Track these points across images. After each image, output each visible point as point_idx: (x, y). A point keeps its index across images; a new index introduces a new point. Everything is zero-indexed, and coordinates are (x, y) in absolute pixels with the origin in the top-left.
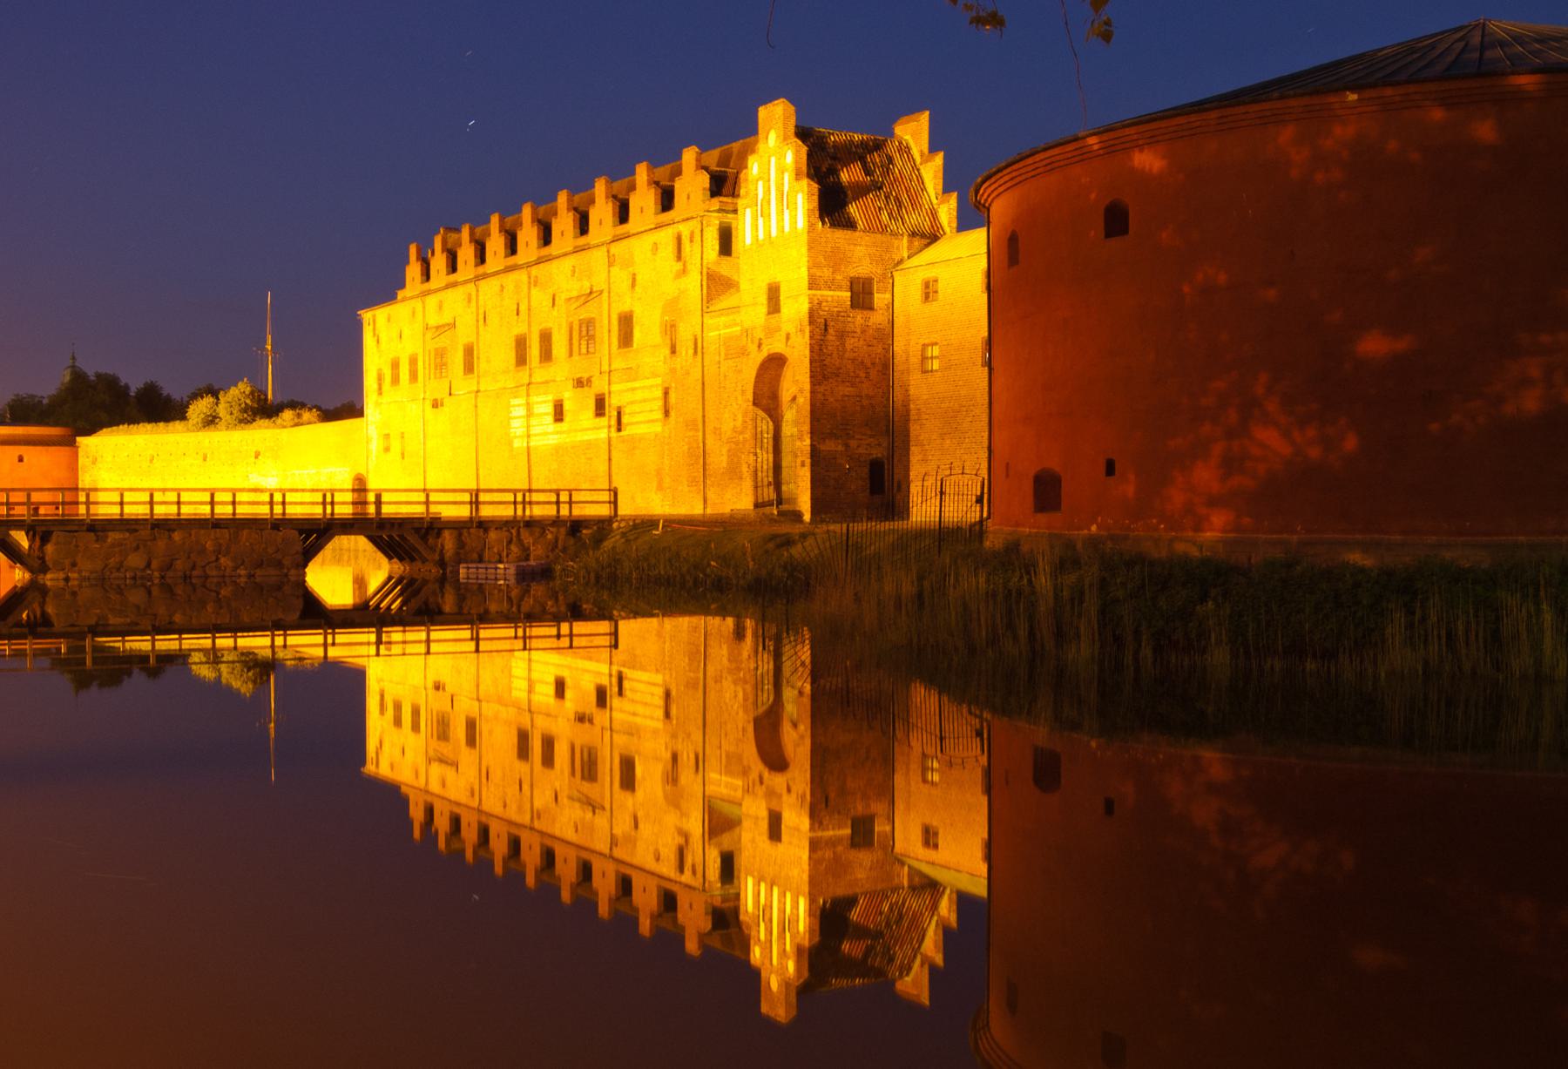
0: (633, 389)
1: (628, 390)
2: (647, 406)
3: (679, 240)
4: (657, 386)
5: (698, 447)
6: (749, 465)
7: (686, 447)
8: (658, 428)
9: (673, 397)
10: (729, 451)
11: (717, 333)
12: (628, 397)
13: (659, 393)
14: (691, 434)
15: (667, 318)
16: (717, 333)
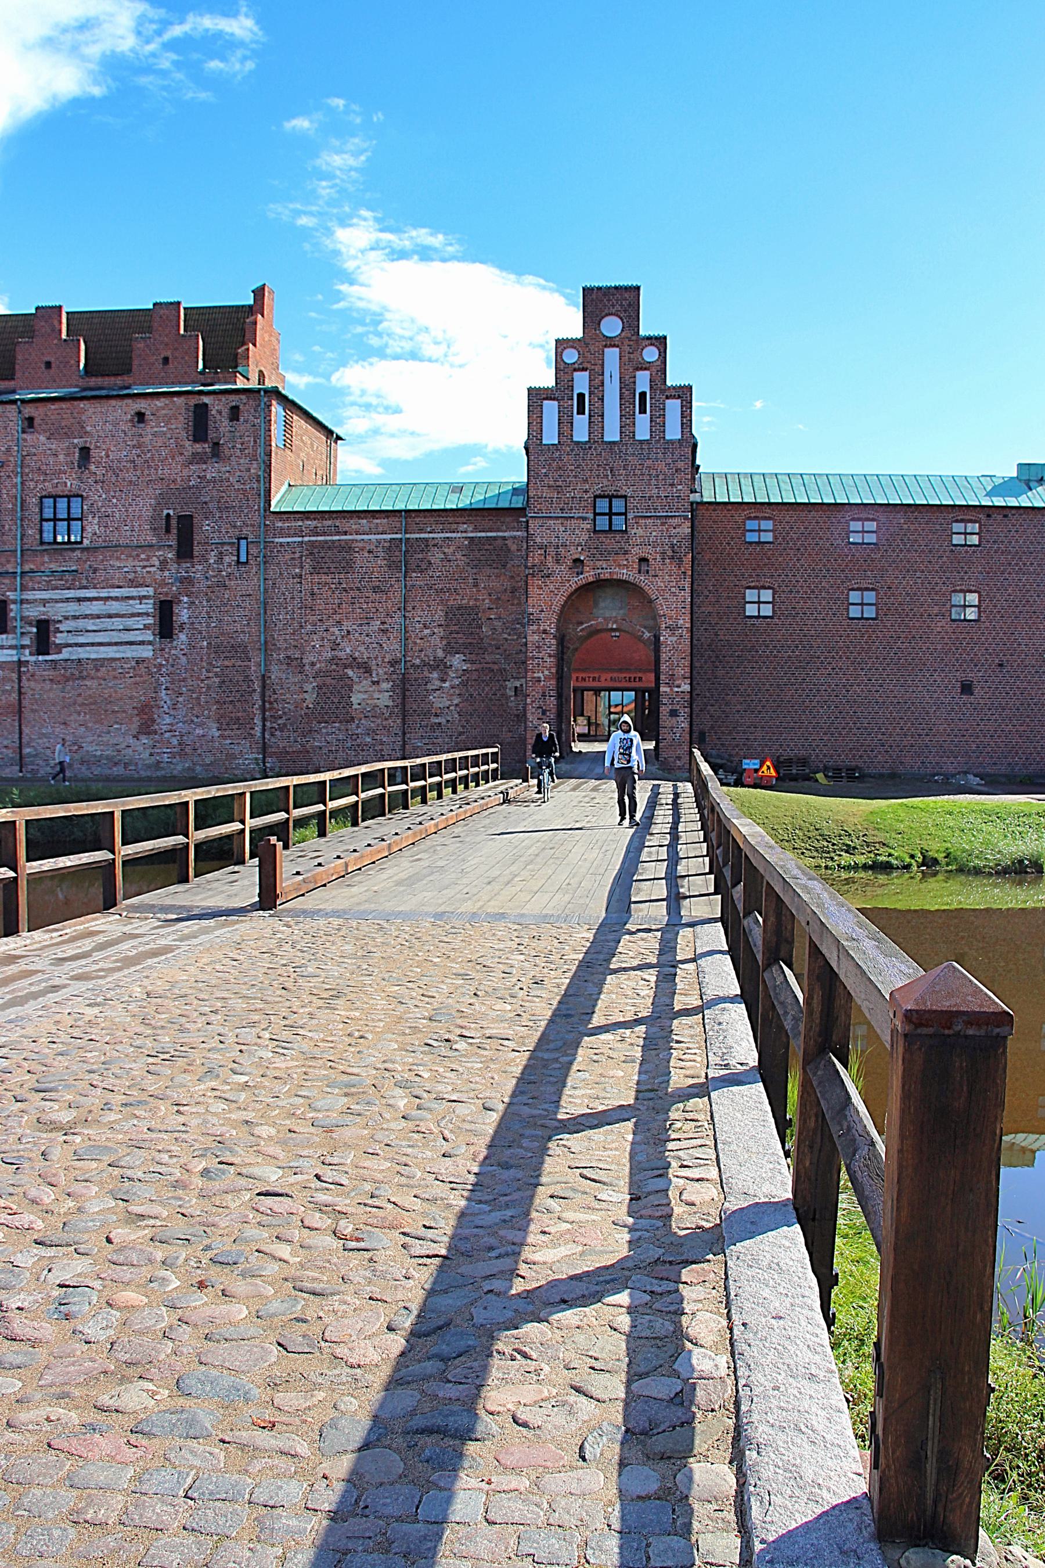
0: (79, 600)
1: (68, 600)
2: (118, 623)
3: (201, 413)
4: (141, 598)
5: (247, 679)
6: (544, 713)
7: (217, 680)
8: (147, 652)
9: (182, 614)
10: (319, 687)
11: (300, 539)
12: (73, 608)
13: (148, 606)
14: (226, 663)
15: (171, 512)
16: (300, 539)
